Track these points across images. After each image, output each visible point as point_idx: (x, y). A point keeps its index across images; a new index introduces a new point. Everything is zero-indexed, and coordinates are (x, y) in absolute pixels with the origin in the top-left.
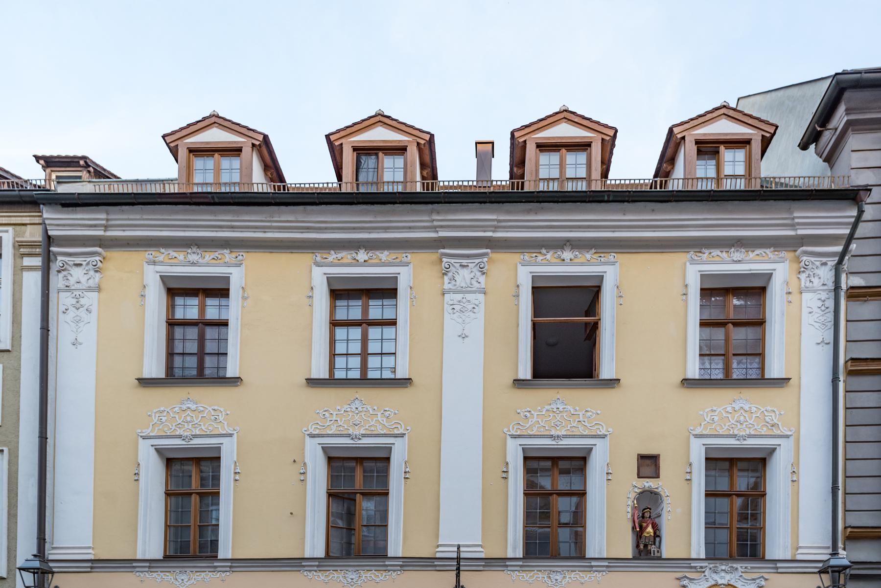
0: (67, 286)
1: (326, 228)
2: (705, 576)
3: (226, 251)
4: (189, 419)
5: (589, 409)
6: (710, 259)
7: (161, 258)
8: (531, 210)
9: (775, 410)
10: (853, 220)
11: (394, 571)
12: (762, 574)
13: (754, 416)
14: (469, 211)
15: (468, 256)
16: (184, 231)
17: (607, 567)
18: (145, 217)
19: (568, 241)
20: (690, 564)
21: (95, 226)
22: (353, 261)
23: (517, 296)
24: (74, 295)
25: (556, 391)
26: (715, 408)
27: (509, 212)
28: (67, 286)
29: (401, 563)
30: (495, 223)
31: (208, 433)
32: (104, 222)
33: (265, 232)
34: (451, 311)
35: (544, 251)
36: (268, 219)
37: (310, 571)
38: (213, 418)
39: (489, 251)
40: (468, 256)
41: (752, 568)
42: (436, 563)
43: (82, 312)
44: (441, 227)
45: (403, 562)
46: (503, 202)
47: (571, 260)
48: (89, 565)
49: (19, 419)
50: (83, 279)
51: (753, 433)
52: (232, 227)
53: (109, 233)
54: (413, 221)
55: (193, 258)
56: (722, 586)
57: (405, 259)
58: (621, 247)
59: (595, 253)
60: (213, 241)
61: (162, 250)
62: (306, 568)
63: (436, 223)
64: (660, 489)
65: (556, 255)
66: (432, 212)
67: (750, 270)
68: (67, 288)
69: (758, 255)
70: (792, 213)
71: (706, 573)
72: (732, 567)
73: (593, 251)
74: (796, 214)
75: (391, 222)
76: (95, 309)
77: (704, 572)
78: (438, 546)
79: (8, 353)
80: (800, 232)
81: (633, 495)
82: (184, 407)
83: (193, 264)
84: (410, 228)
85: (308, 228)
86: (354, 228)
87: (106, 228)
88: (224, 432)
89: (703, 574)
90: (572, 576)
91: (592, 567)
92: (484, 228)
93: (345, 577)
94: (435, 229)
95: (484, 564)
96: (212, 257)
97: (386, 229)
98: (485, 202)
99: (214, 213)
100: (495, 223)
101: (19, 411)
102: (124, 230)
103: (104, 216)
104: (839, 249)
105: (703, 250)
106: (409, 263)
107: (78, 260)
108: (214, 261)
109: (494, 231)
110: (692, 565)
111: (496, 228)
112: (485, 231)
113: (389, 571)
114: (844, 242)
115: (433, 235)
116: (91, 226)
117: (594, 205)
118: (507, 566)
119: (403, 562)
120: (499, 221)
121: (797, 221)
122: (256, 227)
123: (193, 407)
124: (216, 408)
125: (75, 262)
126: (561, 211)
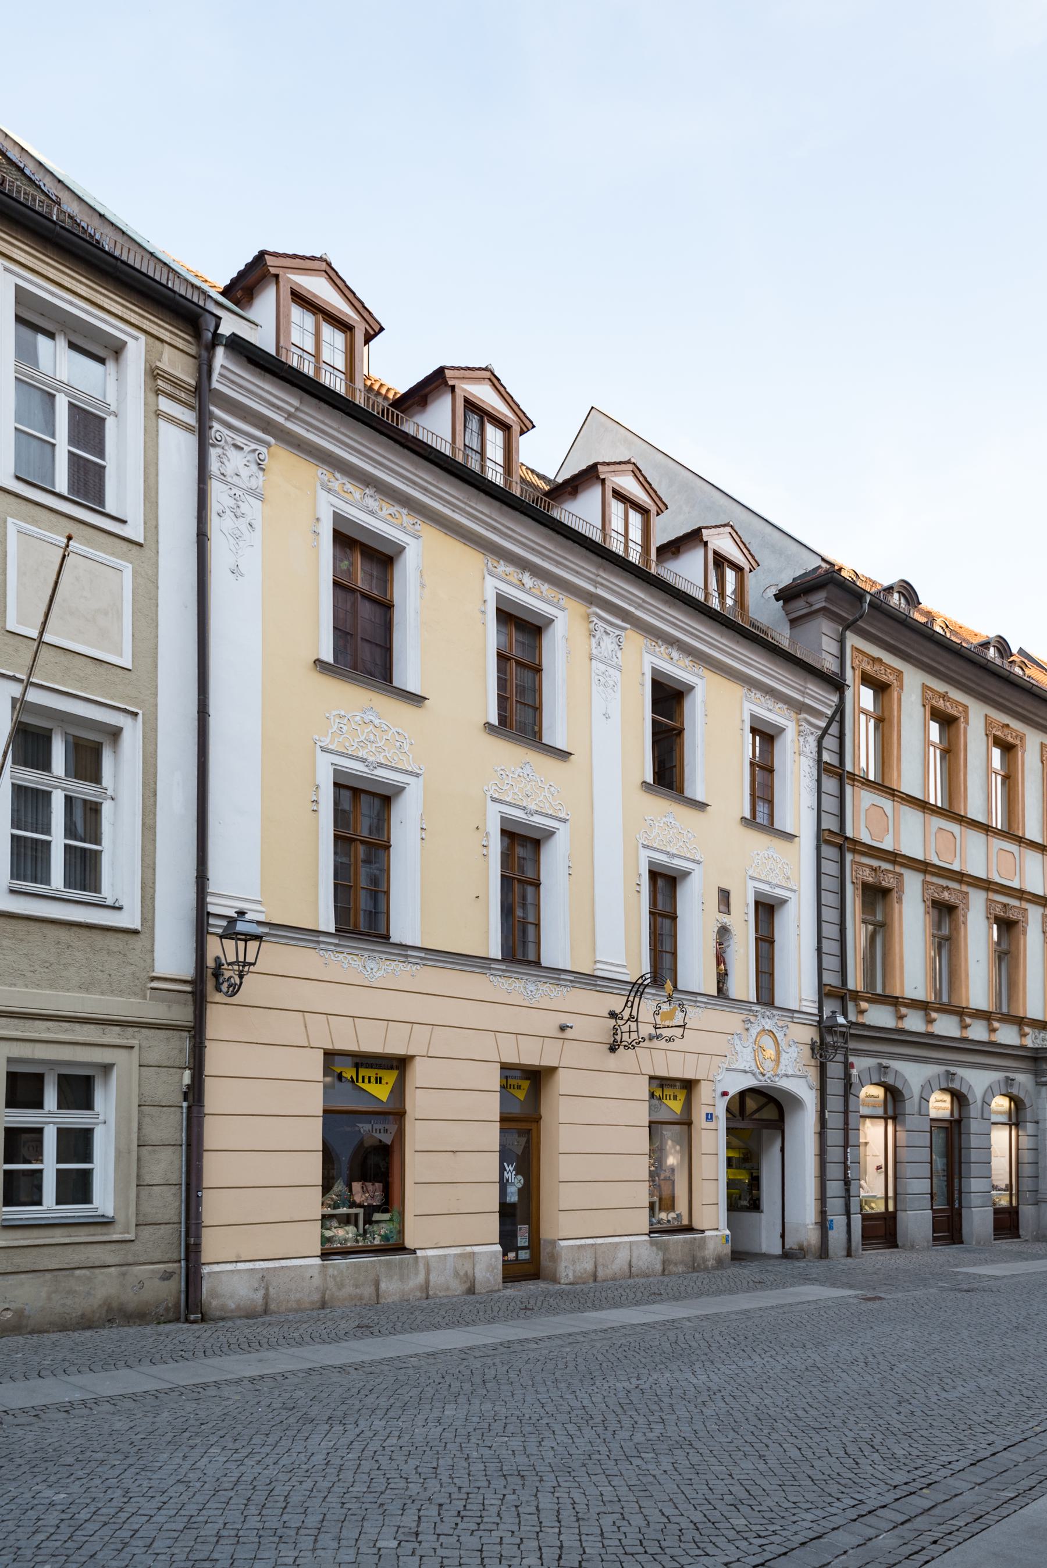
0: (223, 474)
1: (510, 537)
3: (405, 511)
4: (372, 737)
7: (336, 485)
11: (565, 986)
14: (627, 580)
15: (611, 624)
16: (375, 467)
18: (342, 430)
19: (678, 641)
21: (278, 408)
22: (519, 583)
23: (643, 685)
24: (232, 493)
25: (670, 803)
27: (653, 596)
28: (223, 474)
29: (572, 978)
30: (641, 602)
31: (393, 765)
33: (454, 511)
34: (597, 682)
35: (660, 643)
36: (465, 500)
37: (495, 975)
38: (398, 744)
39: (628, 626)
40: (611, 624)
42: (599, 983)
43: (242, 524)
44: (602, 584)
45: (575, 977)
49: (156, 666)
50: (244, 473)
52: (426, 489)
53: (289, 425)
54: (583, 568)
55: (372, 503)
57: (562, 603)
60: (394, 491)
61: (338, 475)
62: (493, 972)
63: (599, 579)
65: (667, 651)
66: (599, 566)
68: (222, 477)
73: (690, 658)
74: (810, 686)
75: (566, 559)
76: (257, 524)
77: (756, 1016)
78: (596, 962)
79: (138, 548)
80: (807, 701)
81: (716, 930)
82: (367, 718)
83: (372, 513)
84: (577, 572)
85: (495, 528)
86: (533, 549)
88: (410, 769)
92: (631, 602)
93: (525, 988)
94: (595, 584)
96: (390, 512)
97: (558, 564)
98: (639, 578)
101: (157, 653)
102: (308, 430)
105: (752, 689)
106: (566, 609)
107: (240, 440)
108: (389, 518)
109: (636, 608)
111: (639, 606)
112: (630, 605)
113: (561, 985)
115: (591, 588)
116: (274, 405)
117: (706, 618)
119: (575, 977)
120: (644, 601)
122: (449, 502)
123: (377, 722)
124: (400, 731)
125: (235, 442)
126: (686, 613)
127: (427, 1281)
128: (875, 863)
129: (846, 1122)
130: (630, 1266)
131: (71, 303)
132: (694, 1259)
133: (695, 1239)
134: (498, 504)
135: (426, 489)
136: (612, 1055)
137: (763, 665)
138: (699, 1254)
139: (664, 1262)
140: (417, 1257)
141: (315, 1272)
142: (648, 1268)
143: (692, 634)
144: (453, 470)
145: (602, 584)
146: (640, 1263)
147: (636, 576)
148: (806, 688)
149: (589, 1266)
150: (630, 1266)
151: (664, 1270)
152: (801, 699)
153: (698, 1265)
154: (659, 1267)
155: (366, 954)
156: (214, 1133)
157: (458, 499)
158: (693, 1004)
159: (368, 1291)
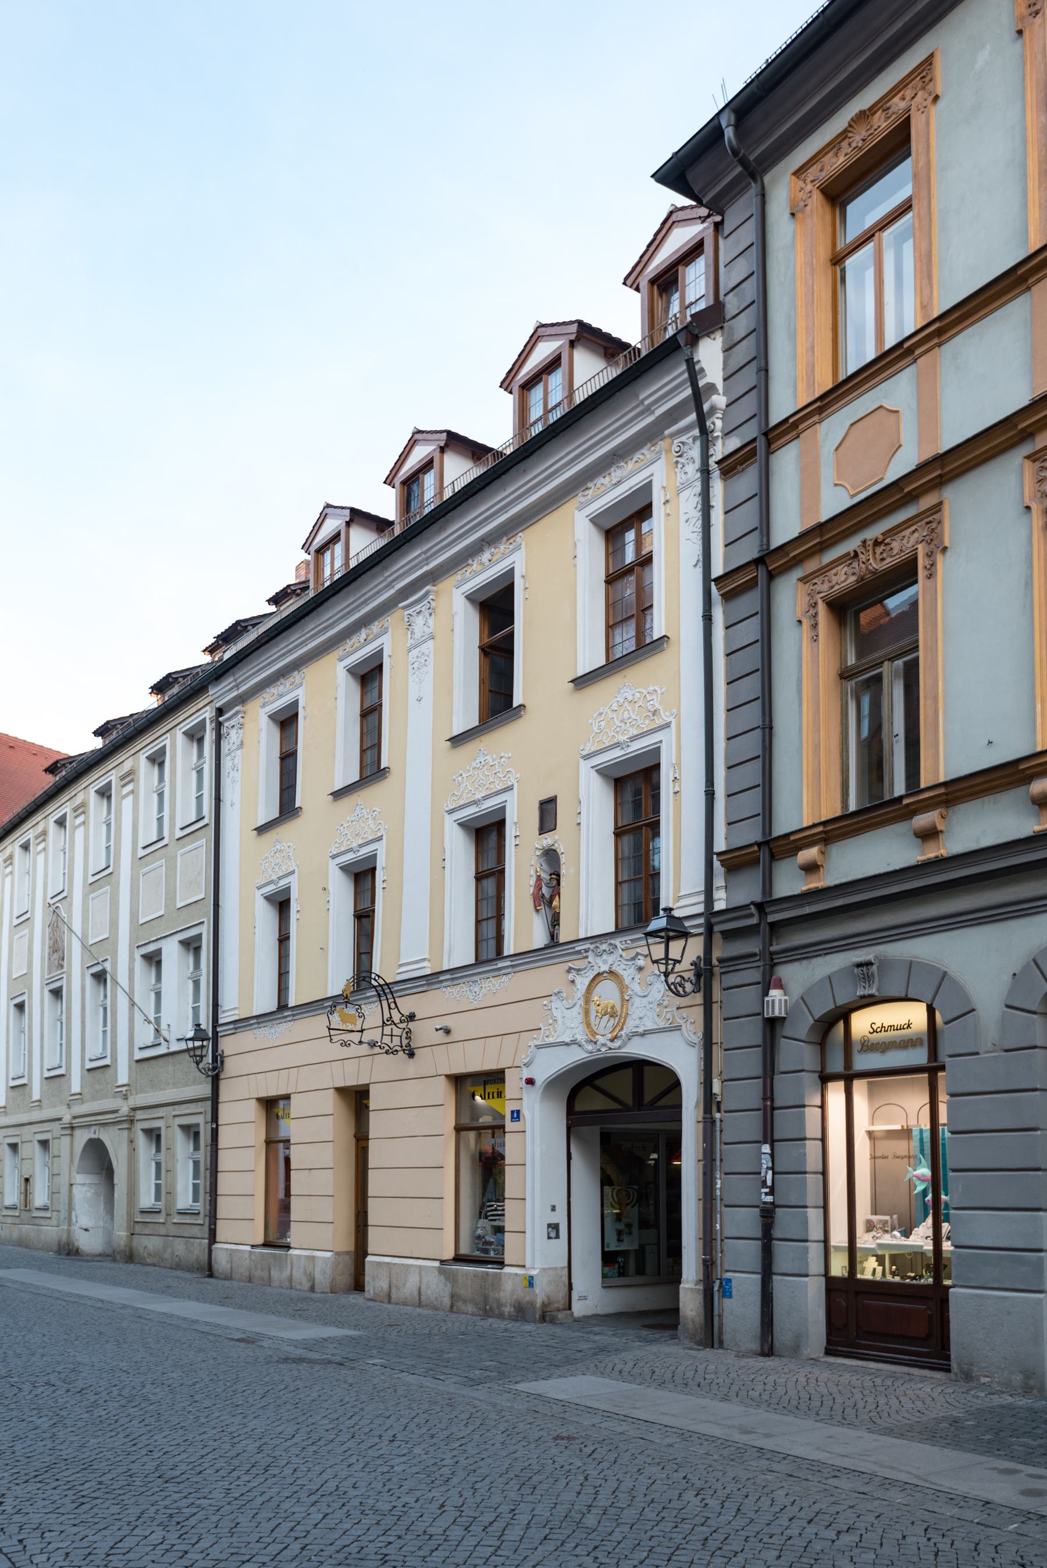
1: (334, 623)
2: (589, 962)
5: (502, 755)
6: (596, 493)
8: (441, 527)
9: (656, 688)
10: (686, 375)
12: (638, 950)
13: (637, 706)
17: (513, 966)
20: (574, 948)
25: (478, 740)
26: (601, 711)
27: (428, 540)
30: (423, 556)
32: (233, 684)
41: (633, 941)
44: (394, 580)
46: (421, 532)
47: (490, 561)
48: (232, 1026)
51: (636, 732)
52: (290, 651)
53: (241, 690)
54: (376, 586)
56: (605, 975)
58: (525, 521)
59: (508, 540)
64: (556, 845)
67: (630, 489)
69: (637, 462)
70: (638, 397)
71: (590, 959)
72: (611, 944)
80: (659, 412)
85: (325, 628)
87: (237, 686)
89: (587, 960)
90: (487, 985)
91: (500, 969)
92: (418, 566)
95: (424, 982)
99: (277, 645)
100: (423, 556)
103: (231, 679)
104: (693, 417)
110: (577, 949)
111: (427, 561)
112: (421, 568)
114: (692, 404)
118: (441, 982)
120: (425, 553)
121: (646, 403)
127: (291, 1275)
128: (852, 544)
129: (768, 1094)
130: (420, 1293)
131: (193, 721)
132: (486, 1299)
133: (487, 1274)
134: (314, 613)
135: (290, 651)
136: (411, 1060)
137: (567, 454)
138: (491, 1294)
139: (453, 1296)
140: (286, 1255)
141: (247, 1256)
142: (436, 1299)
143: (480, 523)
144: (287, 624)
145: (394, 580)
146: (429, 1292)
147: (398, 549)
148: (642, 402)
149: (384, 1285)
150: (420, 1293)
151: (452, 1306)
152: (650, 419)
153: (491, 1309)
154: (447, 1301)
155: (270, 1024)
156: (223, 1164)
157: (300, 637)
158: (497, 973)
159: (266, 1275)
